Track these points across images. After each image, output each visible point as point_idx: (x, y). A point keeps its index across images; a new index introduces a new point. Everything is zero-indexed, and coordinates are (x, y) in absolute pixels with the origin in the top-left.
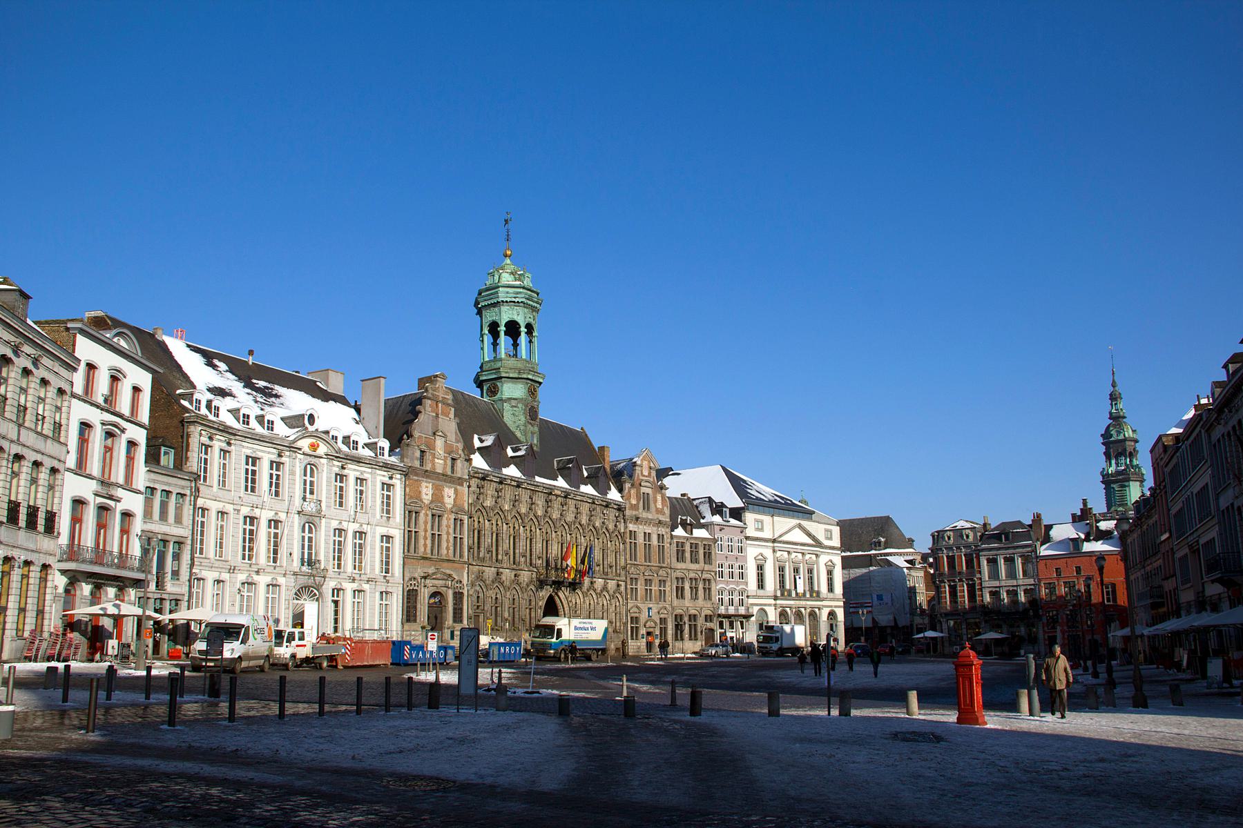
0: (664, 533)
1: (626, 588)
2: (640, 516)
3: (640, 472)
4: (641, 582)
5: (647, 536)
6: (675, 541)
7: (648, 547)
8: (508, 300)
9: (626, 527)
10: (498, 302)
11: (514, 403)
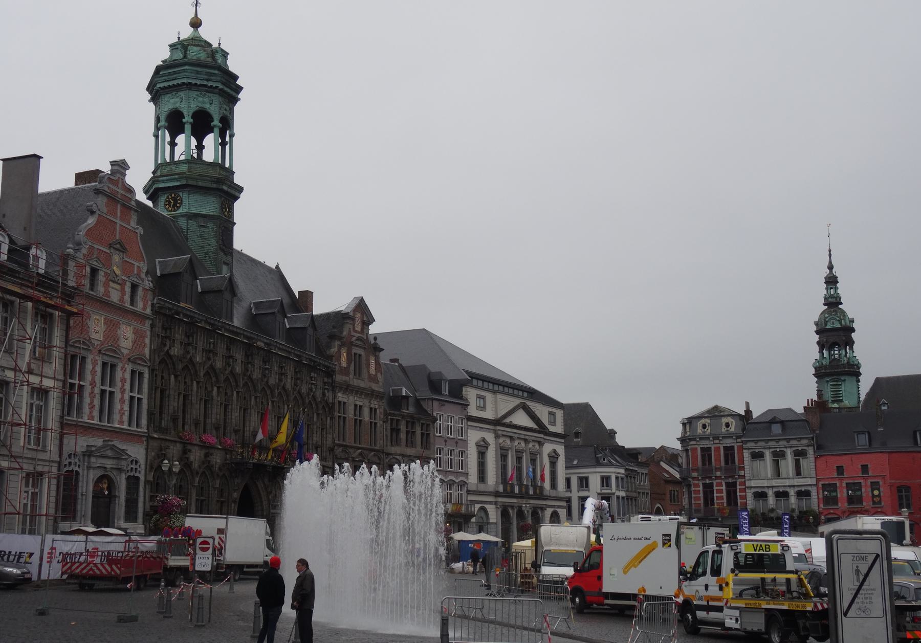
0: (377, 408)
2: (351, 383)
5: (358, 409)
7: (358, 423)
8: (199, 82)
9: (335, 397)
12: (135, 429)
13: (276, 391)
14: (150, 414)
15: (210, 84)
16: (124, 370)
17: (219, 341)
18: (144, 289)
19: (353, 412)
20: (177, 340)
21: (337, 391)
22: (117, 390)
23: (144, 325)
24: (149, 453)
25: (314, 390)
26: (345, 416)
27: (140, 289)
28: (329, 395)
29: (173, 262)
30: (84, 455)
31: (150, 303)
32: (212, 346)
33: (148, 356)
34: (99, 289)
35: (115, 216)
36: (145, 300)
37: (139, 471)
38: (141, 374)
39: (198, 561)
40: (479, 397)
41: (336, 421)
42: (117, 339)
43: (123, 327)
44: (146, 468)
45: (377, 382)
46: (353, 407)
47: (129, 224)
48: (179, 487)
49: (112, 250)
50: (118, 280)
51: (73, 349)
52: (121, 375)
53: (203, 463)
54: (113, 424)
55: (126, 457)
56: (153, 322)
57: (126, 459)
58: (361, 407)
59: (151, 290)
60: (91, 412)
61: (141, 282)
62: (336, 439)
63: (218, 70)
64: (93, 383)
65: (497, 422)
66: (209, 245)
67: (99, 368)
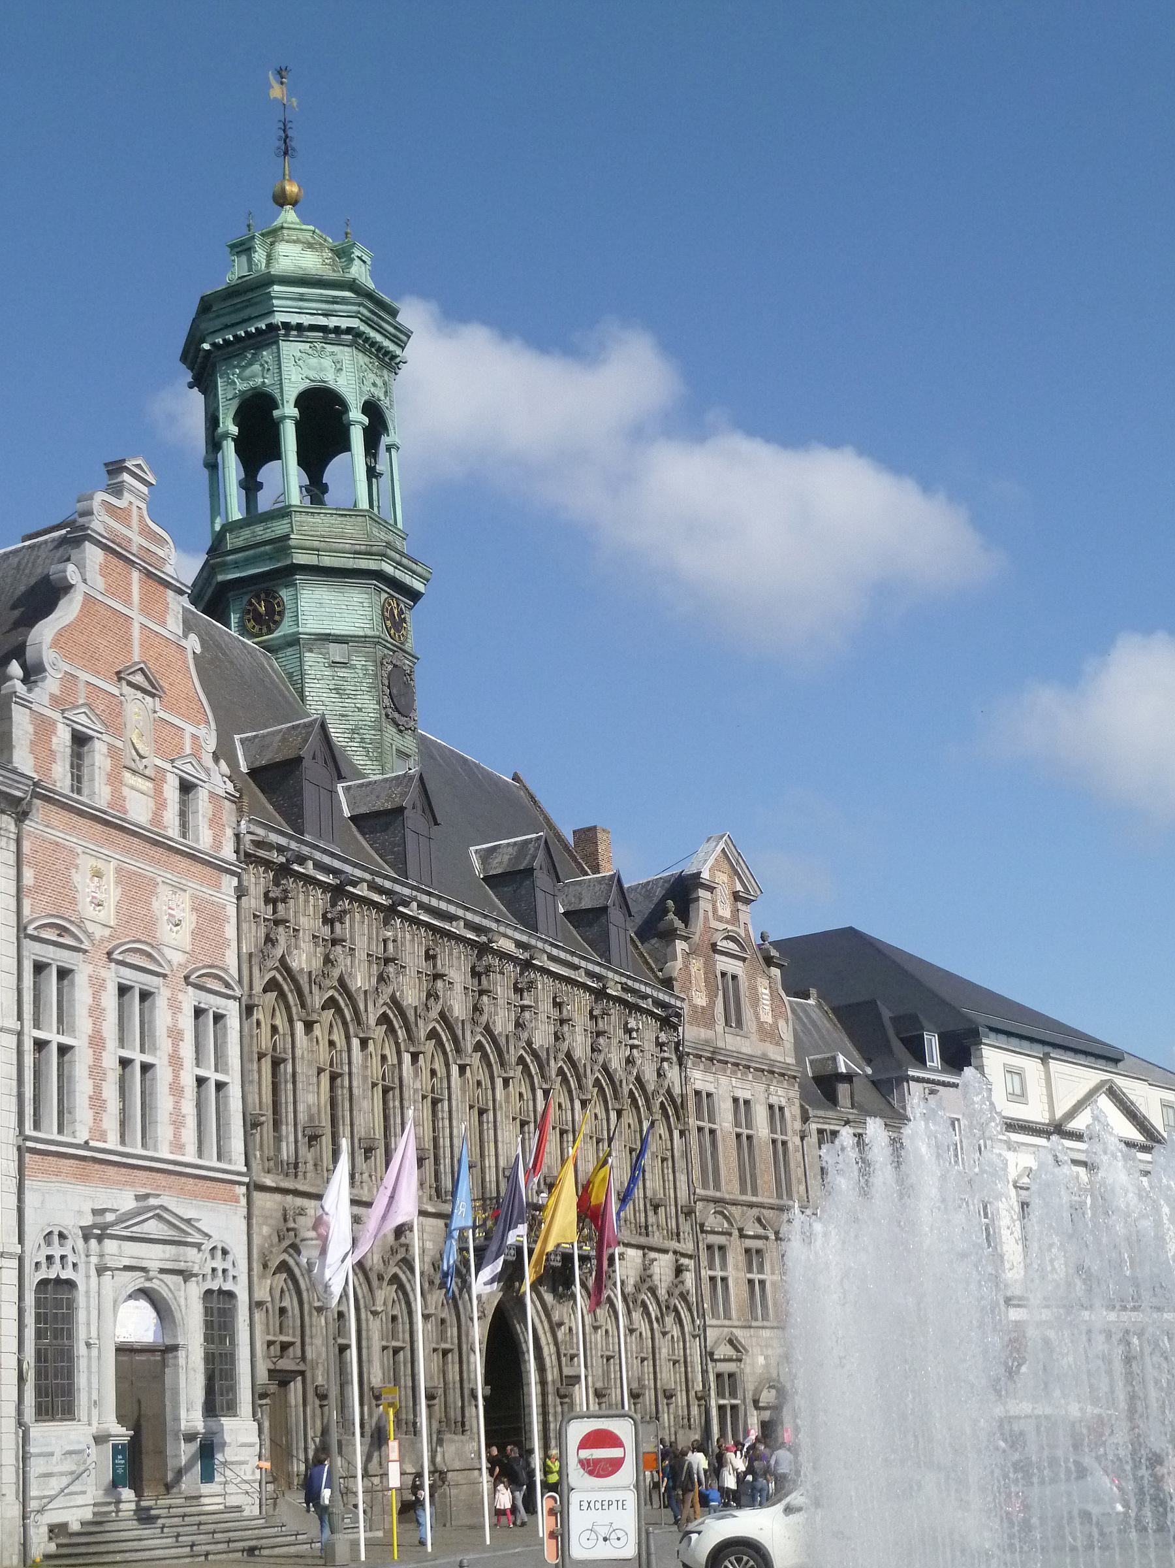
0: (783, 1104)
1: (698, 1278)
2: (721, 1044)
3: (709, 908)
4: (735, 1257)
5: (742, 1107)
6: (814, 1127)
7: (745, 1142)
8: (306, 320)
9: (685, 1080)
10: (272, 327)
11: (336, 652)
12: (215, 1163)
13: (552, 1062)
14: (251, 1124)
15: (332, 322)
16: (175, 1006)
17: (408, 936)
18: (212, 795)
19: (730, 1116)
20: (304, 929)
21: (690, 1064)
22: (160, 1059)
23: (218, 887)
24: (255, 1227)
25: (639, 1062)
26: (714, 1126)
27: (202, 795)
28: (673, 1073)
29: (279, 737)
30: (86, 1238)
31: (229, 833)
32: (390, 946)
33: (234, 972)
34: (97, 791)
35: (128, 602)
36: (215, 822)
37: (234, 1277)
38: (218, 1018)
39: (578, 1520)
40: (1010, 1071)
41: (694, 1136)
42: (151, 924)
43: (164, 892)
44: (250, 1270)
45: (778, 1041)
46: (729, 1104)
47: (163, 624)
48: (336, 1316)
49: (127, 690)
50: (146, 767)
51: (37, 947)
52: (169, 1019)
53: (393, 1251)
54: (156, 1150)
55: (196, 1238)
56: (239, 882)
57: (198, 1246)
58: (747, 1102)
59: (229, 797)
60: (97, 1118)
61: (203, 776)
62: (697, 1183)
63: (351, 290)
64: (97, 1042)
65: (1058, 1129)
66: (360, 710)
67: (110, 999)
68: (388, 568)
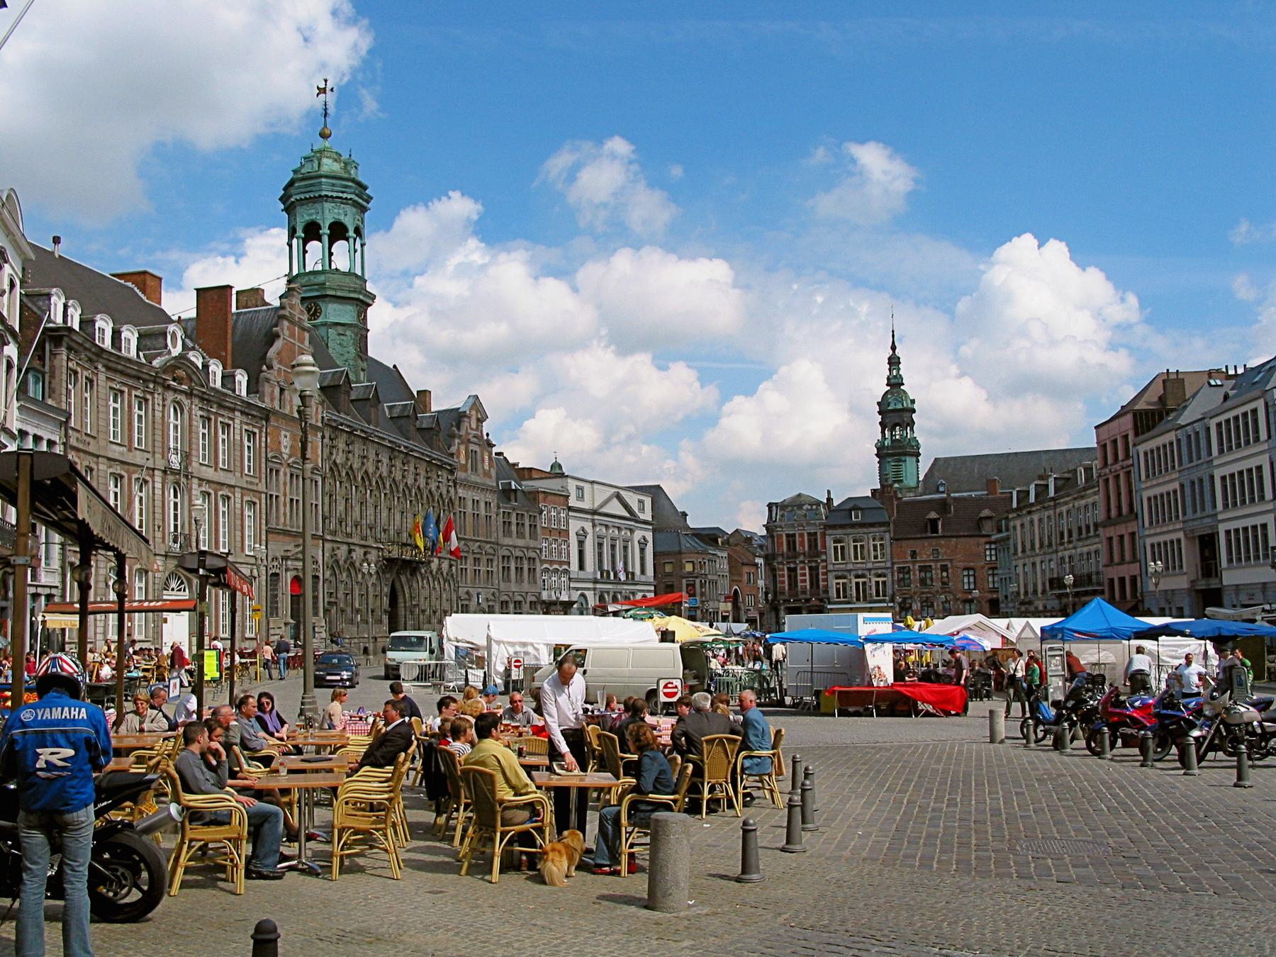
8: (335, 194)
9: (456, 492)
11: (340, 330)
15: (345, 195)
38: (316, 482)
45: (490, 477)
68: (361, 297)
